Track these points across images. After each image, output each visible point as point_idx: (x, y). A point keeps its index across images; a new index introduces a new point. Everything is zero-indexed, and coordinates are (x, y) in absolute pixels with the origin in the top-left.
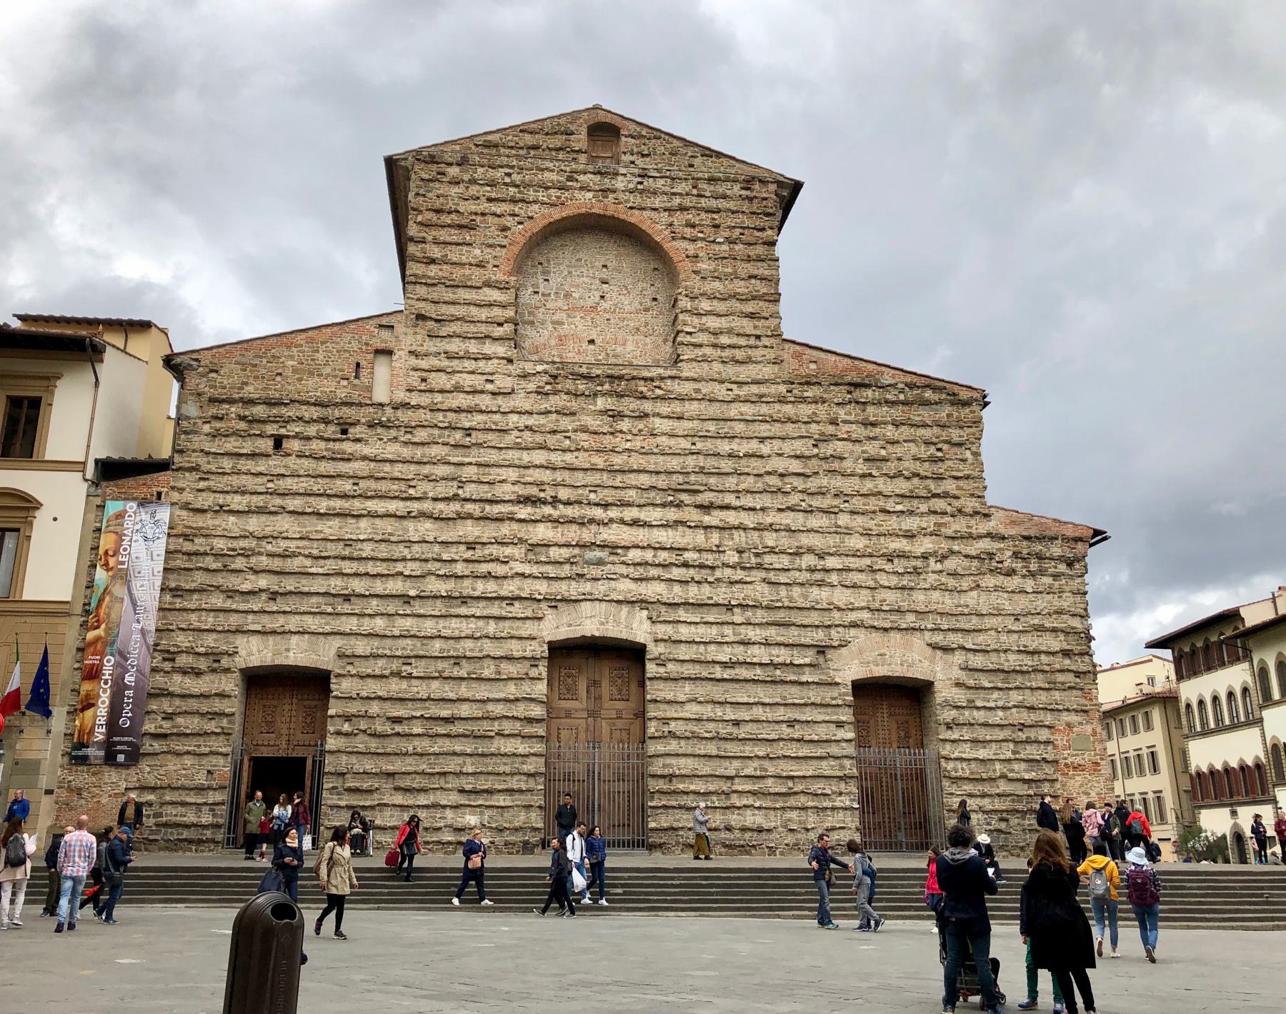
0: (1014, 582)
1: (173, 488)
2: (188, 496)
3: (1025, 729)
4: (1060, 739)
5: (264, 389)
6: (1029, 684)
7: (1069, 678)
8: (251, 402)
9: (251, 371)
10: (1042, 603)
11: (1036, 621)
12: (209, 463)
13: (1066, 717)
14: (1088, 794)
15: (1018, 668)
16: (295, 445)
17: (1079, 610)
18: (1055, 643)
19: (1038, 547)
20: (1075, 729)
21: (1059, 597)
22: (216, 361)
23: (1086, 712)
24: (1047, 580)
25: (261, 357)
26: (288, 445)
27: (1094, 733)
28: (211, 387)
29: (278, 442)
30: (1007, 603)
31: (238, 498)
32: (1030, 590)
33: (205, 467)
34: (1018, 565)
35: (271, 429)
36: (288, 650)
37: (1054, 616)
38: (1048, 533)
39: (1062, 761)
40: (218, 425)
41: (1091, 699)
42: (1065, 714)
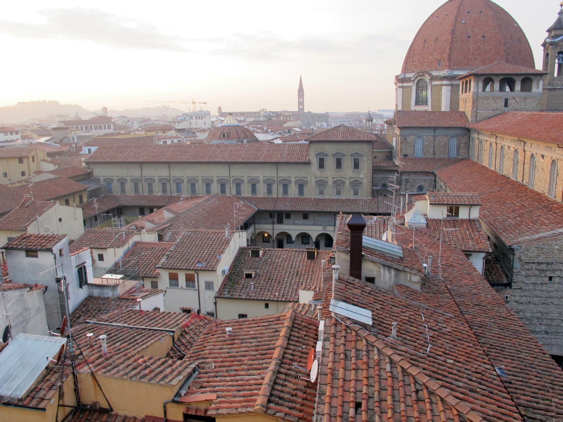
1: (512, 295)
2: (517, 298)
5: (546, 258)
8: (542, 263)
9: (541, 251)
12: (525, 286)
16: (557, 280)
22: (527, 247)
25: (545, 245)
26: (553, 279)
28: (525, 257)
29: (551, 278)
31: (535, 299)
33: (524, 288)
35: (549, 274)
36: (551, 350)
40: (528, 272)
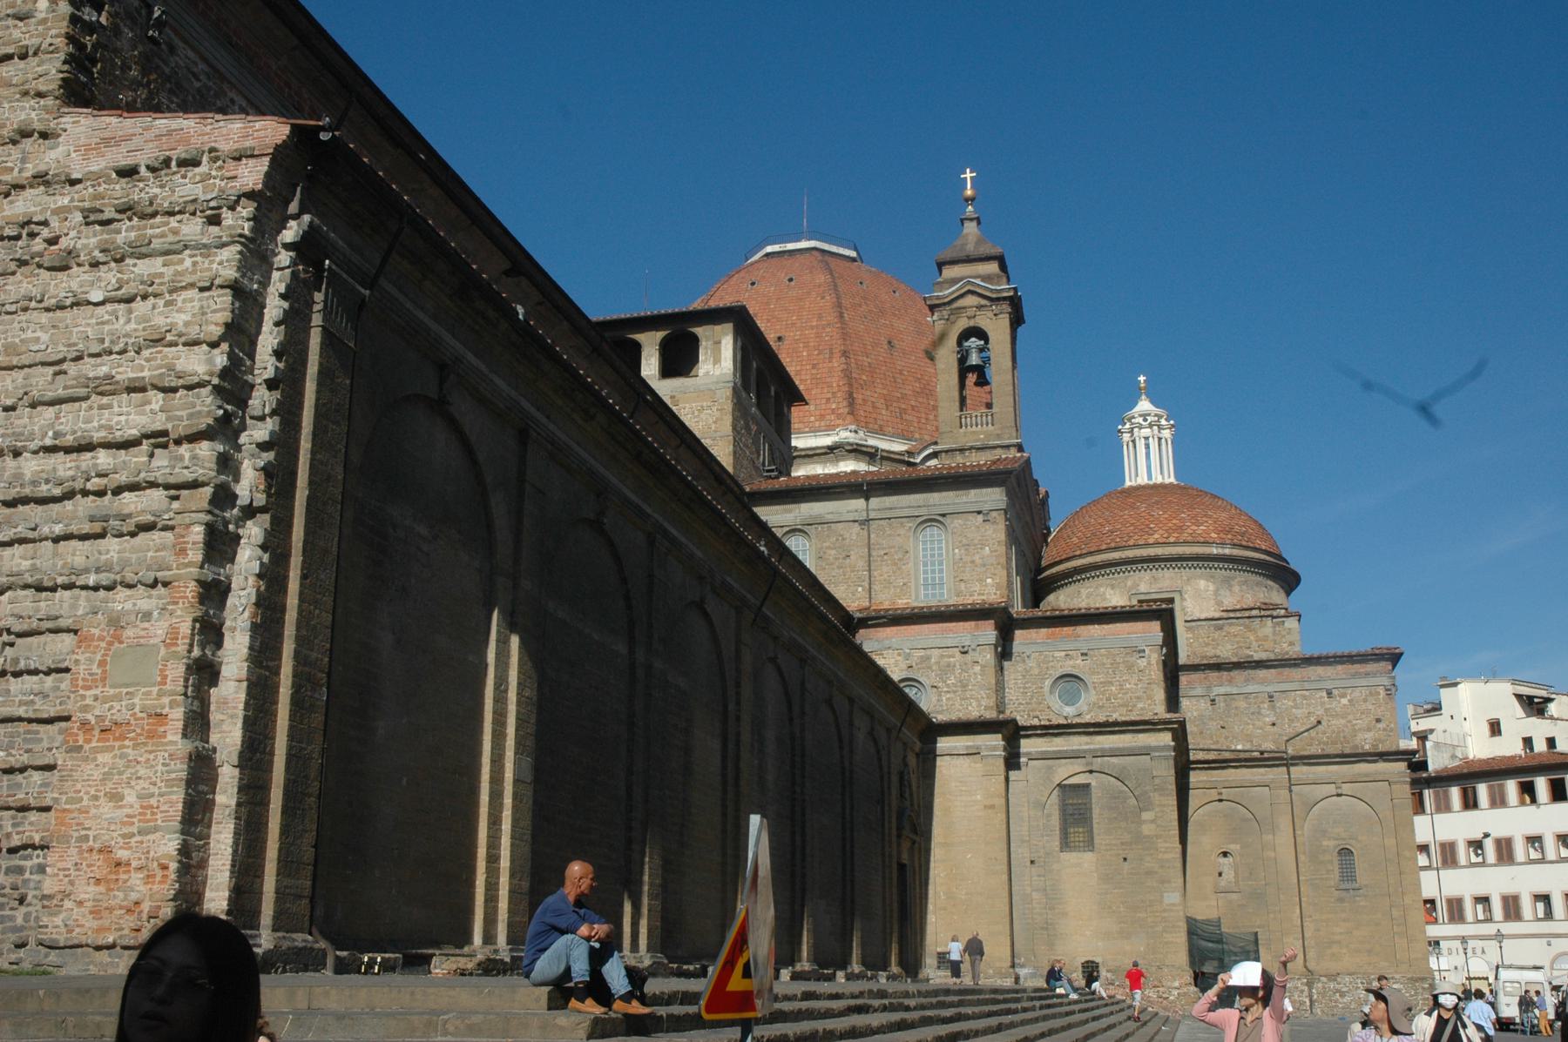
0: (76, 280)
3: (19, 641)
4: (85, 663)
6: (45, 530)
7: (155, 498)
10: (128, 324)
11: (104, 370)
13: (122, 601)
14: (116, 797)
15: (27, 491)
17: (212, 328)
18: (129, 417)
19: (148, 190)
20: (129, 632)
21: (168, 304)
23: (165, 584)
24: (144, 268)
27: (173, 633)
30: (45, 337)
32: (96, 296)
34: (89, 241)
37: (146, 353)
38: (179, 152)
39: (77, 716)
41: (183, 551)
42: (122, 593)
